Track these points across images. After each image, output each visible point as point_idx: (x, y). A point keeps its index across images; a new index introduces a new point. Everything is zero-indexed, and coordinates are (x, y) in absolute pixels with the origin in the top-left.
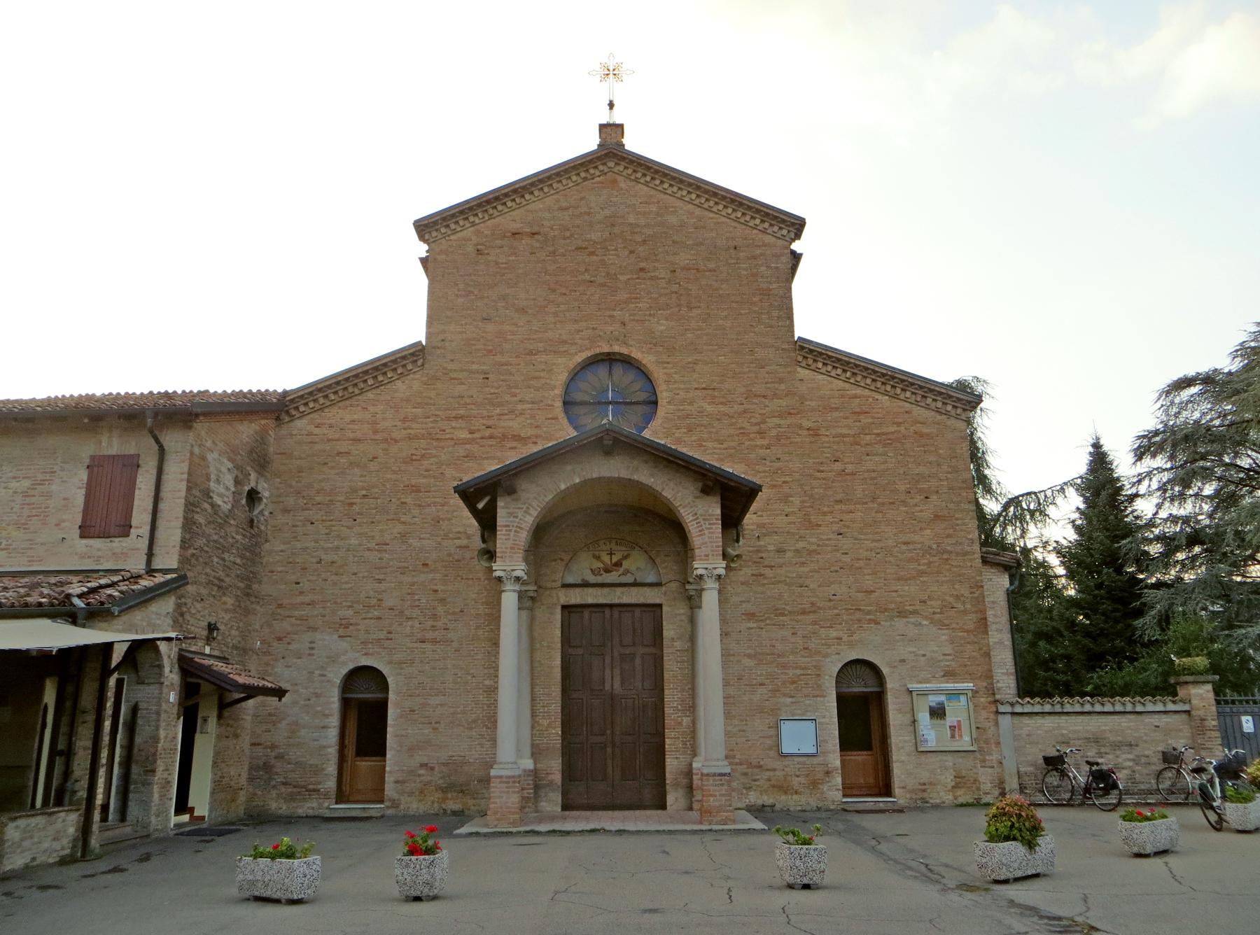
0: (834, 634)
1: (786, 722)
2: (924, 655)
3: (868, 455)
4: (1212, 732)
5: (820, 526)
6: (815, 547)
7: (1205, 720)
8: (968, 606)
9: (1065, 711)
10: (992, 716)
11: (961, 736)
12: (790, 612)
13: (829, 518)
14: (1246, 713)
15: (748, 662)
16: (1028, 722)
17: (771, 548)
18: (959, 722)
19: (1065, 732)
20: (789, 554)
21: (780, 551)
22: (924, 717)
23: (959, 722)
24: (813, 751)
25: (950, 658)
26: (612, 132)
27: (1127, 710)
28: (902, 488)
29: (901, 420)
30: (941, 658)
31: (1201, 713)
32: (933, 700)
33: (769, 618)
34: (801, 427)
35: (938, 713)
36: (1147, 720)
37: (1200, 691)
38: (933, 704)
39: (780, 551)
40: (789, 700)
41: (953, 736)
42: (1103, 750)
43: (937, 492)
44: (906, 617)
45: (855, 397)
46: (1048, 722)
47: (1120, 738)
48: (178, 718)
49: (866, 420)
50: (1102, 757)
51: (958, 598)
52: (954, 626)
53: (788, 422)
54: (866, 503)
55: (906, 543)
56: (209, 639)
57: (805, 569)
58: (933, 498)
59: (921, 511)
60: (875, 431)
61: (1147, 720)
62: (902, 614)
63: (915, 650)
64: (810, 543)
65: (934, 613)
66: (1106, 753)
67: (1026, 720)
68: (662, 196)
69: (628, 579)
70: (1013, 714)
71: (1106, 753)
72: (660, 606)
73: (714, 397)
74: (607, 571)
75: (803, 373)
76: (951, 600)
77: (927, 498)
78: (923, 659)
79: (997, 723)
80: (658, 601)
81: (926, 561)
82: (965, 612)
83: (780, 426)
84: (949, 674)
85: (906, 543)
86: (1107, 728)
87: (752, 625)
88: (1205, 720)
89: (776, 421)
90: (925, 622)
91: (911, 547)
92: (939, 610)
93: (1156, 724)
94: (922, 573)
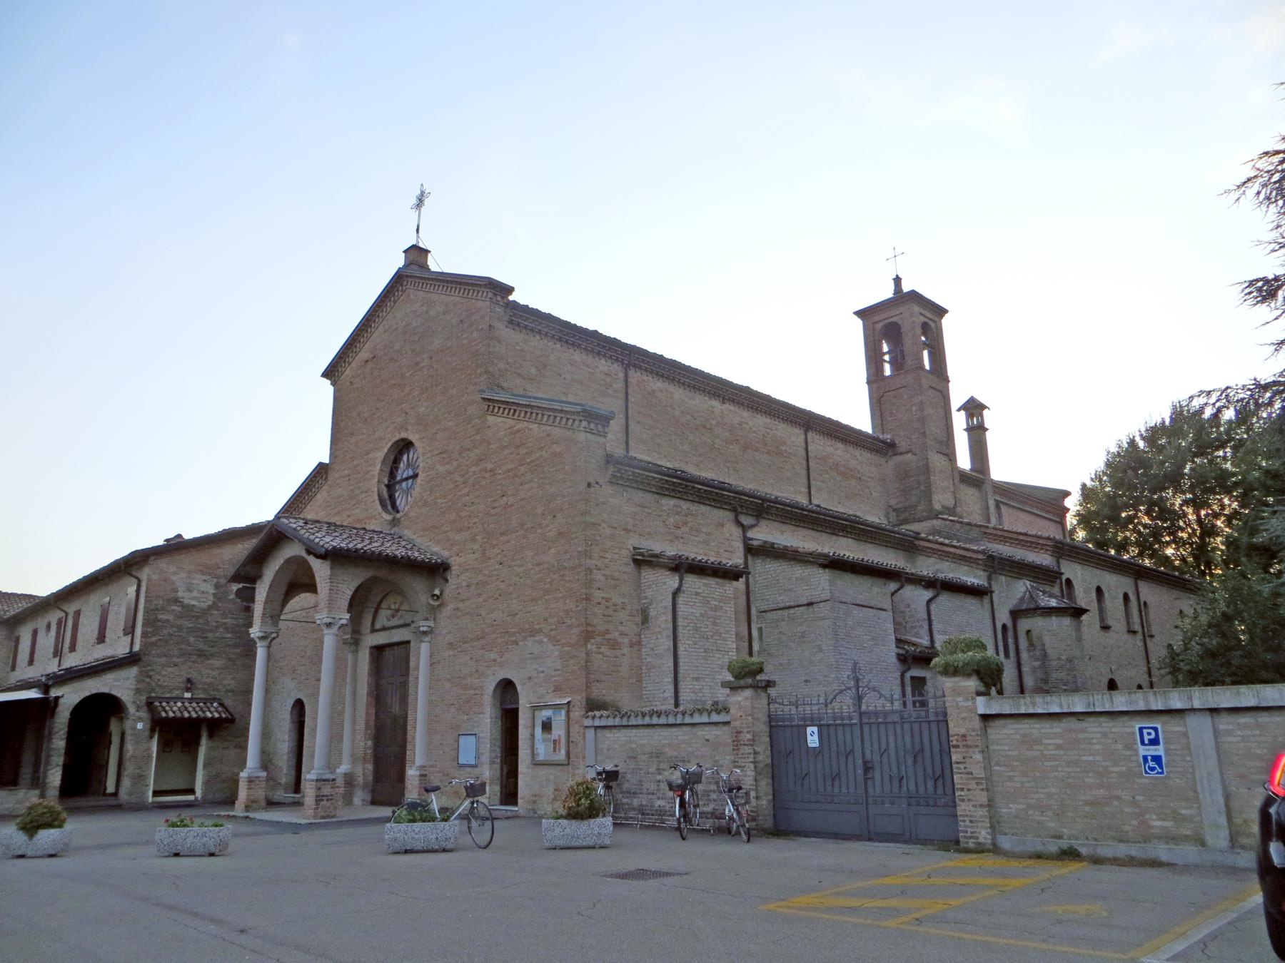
0: (493, 656)
1: (463, 737)
2: (543, 672)
3: (522, 485)
4: (746, 747)
5: (490, 558)
6: (486, 579)
7: (741, 732)
8: (574, 620)
9: (630, 723)
10: (582, 730)
11: (560, 750)
12: (471, 639)
13: (496, 551)
14: (144, 726)
15: (448, 685)
16: (609, 735)
17: (464, 584)
18: (559, 736)
19: (634, 746)
20: (473, 587)
21: (468, 586)
22: (538, 730)
23: (559, 736)
24: (473, 762)
25: (559, 672)
26: (416, 254)
27: (678, 722)
28: (539, 511)
29: (543, 445)
30: (553, 673)
31: (737, 724)
32: (546, 714)
33: (460, 646)
34: (486, 471)
35: (547, 726)
36: (699, 733)
37: (739, 699)
38: (544, 719)
39: (468, 586)
40: (466, 717)
41: (555, 750)
42: (662, 766)
43: (562, 509)
44: (534, 636)
45: (519, 431)
46: (622, 735)
47: (676, 753)
48: (151, 737)
49: (523, 451)
50: (660, 774)
51: (567, 612)
52: (563, 641)
53: (479, 468)
54: (517, 531)
55: (539, 565)
56: (188, 690)
57: (481, 599)
58: (559, 515)
59: (550, 531)
60: (528, 460)
61: (699, 733)
62: (533, 633)
63: (537, 666)
64: (485, 575)
65: (551, 630)
66: (664, 770)
67: (608, 734)
68: (430, 295)
69: (401, 622)
70: (596, 728)
71: (664, 770)
72: (408, 642)
73: (444, 458)
74: (393, 617)
75: (491, 419)
76: (563, 615)
77: (554, 517)
78: (542, 675)
79: (584, 737)
80: (406, 639)
81: (549, 580)
82: (570, 627)
83: (475, 473)
84: (557, 689)
85: (539, 565)
86: (667, 742)
87: (451, 653)
88: (741, 732)
89: (474, 469)
90: (546, 640)
91: (542, 567)
92: (554, 627)
93: (707, 737)
94: (547, 592)
